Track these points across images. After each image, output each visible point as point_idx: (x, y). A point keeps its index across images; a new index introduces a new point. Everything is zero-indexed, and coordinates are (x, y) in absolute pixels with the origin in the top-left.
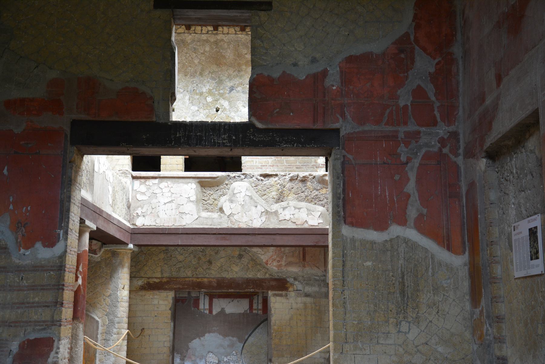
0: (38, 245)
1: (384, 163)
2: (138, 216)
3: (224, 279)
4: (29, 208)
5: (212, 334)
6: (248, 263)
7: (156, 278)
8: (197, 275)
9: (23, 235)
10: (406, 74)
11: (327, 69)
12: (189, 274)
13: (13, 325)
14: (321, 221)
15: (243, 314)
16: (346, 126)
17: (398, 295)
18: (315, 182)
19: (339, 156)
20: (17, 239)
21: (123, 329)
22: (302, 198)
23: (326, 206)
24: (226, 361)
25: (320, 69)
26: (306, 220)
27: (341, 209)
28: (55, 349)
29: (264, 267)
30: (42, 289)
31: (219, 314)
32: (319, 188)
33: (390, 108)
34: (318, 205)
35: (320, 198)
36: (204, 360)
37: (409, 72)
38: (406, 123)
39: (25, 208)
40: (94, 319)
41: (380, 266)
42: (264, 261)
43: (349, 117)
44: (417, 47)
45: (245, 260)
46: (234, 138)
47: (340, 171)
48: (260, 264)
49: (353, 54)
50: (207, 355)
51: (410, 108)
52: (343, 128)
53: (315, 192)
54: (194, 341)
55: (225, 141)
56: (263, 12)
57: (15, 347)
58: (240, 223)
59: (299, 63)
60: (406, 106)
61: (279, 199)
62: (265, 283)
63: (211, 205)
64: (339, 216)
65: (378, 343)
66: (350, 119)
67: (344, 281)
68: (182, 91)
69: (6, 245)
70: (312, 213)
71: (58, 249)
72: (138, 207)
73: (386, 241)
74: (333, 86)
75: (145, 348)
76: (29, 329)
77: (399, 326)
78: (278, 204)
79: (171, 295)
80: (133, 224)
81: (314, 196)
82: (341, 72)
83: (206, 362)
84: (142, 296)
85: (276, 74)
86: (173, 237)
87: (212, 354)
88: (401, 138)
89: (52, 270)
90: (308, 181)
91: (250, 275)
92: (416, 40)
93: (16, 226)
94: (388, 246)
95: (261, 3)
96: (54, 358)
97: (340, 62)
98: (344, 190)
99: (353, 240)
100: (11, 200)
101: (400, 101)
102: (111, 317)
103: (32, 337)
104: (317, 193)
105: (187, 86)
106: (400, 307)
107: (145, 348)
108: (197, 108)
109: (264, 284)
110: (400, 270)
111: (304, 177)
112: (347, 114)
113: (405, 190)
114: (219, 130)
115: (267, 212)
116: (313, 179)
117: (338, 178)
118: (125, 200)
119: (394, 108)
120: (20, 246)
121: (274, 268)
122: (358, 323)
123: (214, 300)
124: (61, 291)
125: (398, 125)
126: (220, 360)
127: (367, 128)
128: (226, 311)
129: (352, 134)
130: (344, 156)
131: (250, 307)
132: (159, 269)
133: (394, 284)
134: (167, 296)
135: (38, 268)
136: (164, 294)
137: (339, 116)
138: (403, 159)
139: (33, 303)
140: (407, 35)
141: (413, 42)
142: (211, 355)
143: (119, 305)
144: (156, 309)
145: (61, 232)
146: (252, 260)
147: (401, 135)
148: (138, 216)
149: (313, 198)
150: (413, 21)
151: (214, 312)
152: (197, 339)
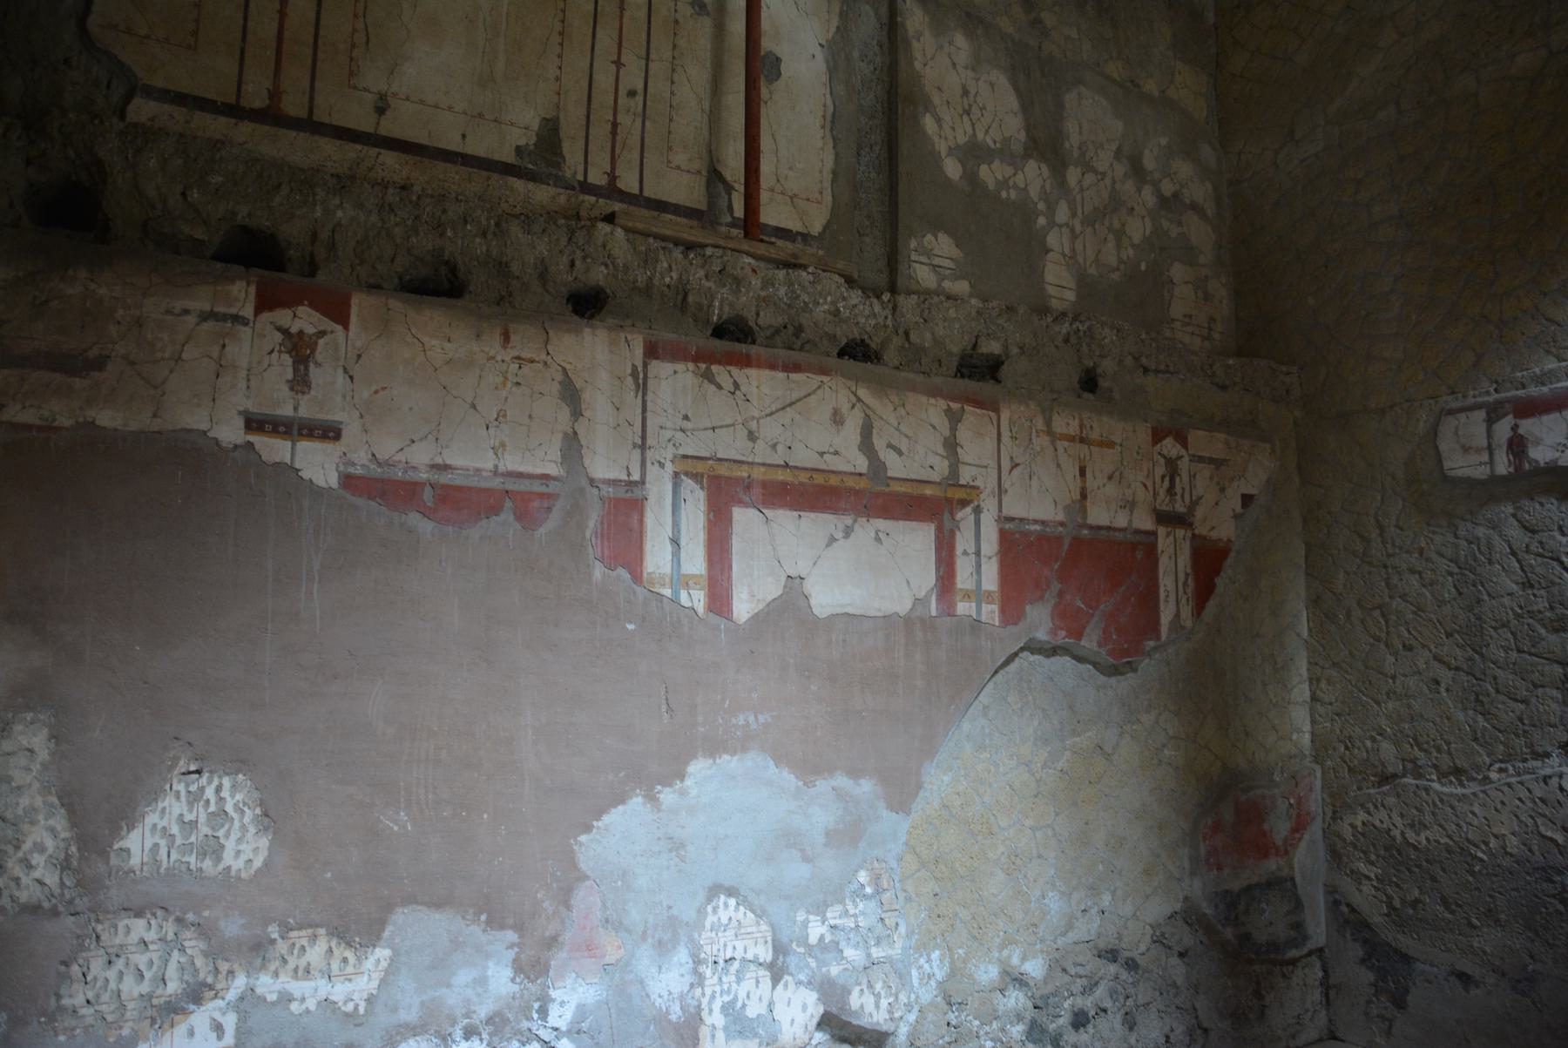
5: (730, 762)
15: (908, 621)
24: (822, 938)
50: (701, 912)
54: (615, 818)
83: (698, 962)
87: (732, 902)
123: (744, 518)
126: (785, 940)
128: (813, 602)
131: (939, 578)
152: (637, 802)
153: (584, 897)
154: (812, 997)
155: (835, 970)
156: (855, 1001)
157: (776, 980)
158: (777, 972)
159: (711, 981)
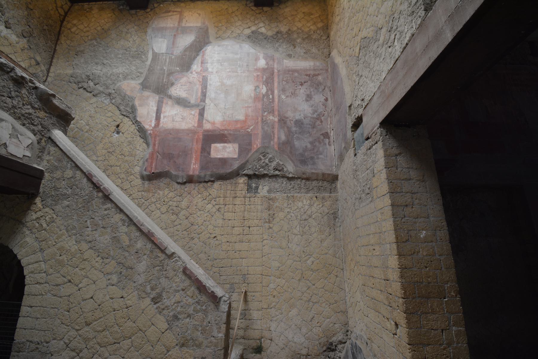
14: (28, 154)
18: (34, 96)
22: (5, 105)
23: (37, 135)
26: (5, 144)
32: (36, 106)
34: (27, 128)
35: (33, 120)
53: (29, 109)
70: (19, 136)
81: (26, 113)
90: (25, 87)
104: (31, 111)
111: (22, 77)
116: (33, 89)
149: (23, 115)
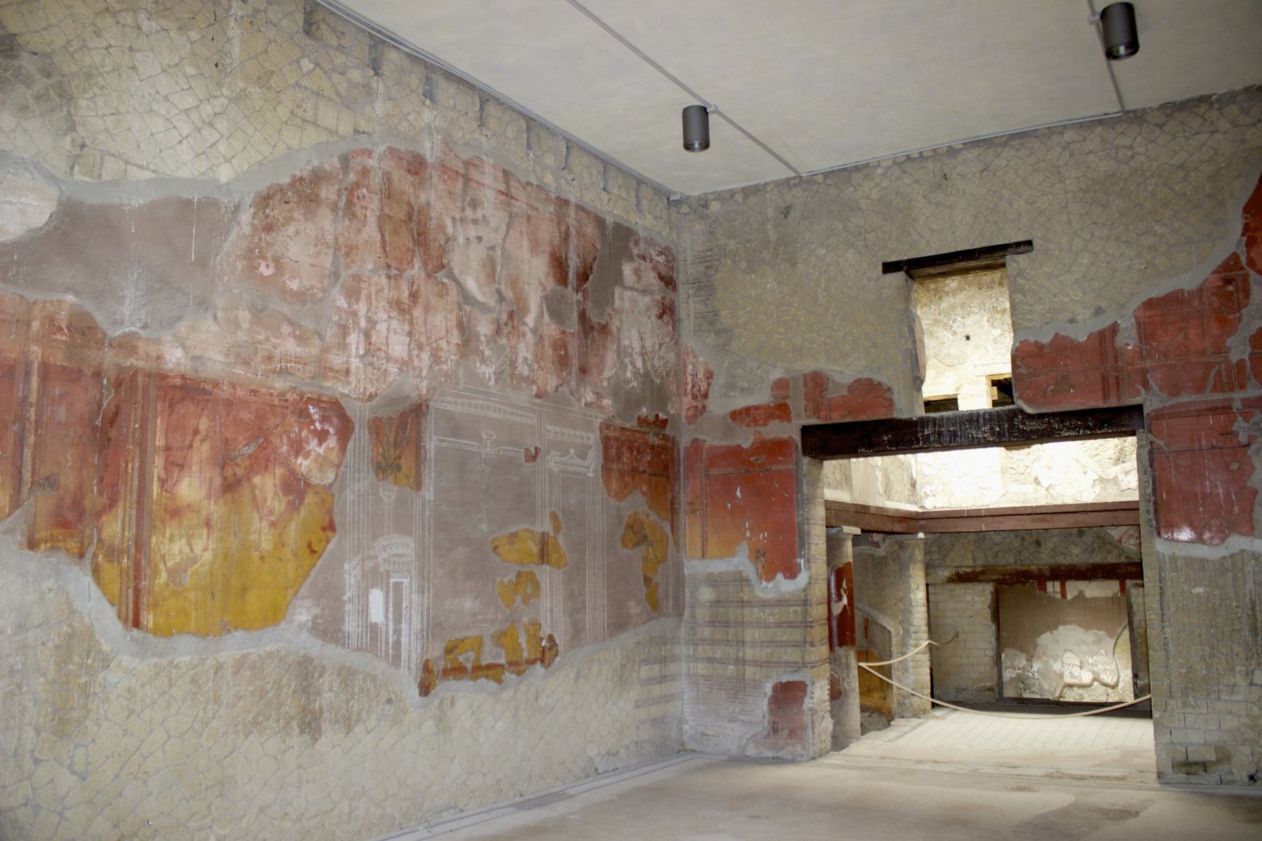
0: (780, 576)
1: (1213, 447)
2: (927, 495)
3: (1059, 566)
4: (766, 535)
5: (1067, 626)
6: (1093, 542)
7: (967, 567)
8: (1021, 561)
9: (763, 566)
10: (1238, 315)
11: (1116, 322)
12: (1011, 560)
13: (764, 665)
15: (1112, 598)
16: (1151, 400)
17: (1247, 634)
19: (1144, 442)
20: (757, 570)
21: (922, 639)
25: (1108, 323)
27: (1152, 516)
28: (809, 694)
29: (1117, 547)
30: (789, 627)
31: (1075, 599)
33: (1217, 367)
36: (1059, 661)
37: (1244, 311)
38: (1242, 386)
39: (761, 535)
40: (885, 628)
41: (1216, 592)
42: (1116, 538)
43: (1154, 386)
44: (1252, 273)
45: (1089, 537)
46: (998, 429)
47: (1147, 464)
48: (1111, 543)
49: (1153, 295)
51: (1248, 364)
52: (1148, 403)
54: (1044, 635)
55: (986, 435)
56: (1022, 256)
57: (768, 688)
58: (1065, 498)
59: (1078, 318)
60: (1241, 363)
61: (1118, 460)
62: (1121, 569)
63: (1022, 474)
64: (1151, 526)
65: (1219, 699)
66: (1157, 389)
67: (1163, 615)
68: (976, 310)
69: (748, 576)
71: (802, 579)
72: (926, 484)
73: (1224, 558)
74: (1128, 345)
75: (961, 657)
76: (781, 670)
77: (1250, 677)
78: (1118, 467)
79: (989, 588)
80: (922, 507)
82: (1138, 324)
83: (1063, 663)
84: (950, 590)
85: (1046, 339)
86: (974, 520)
88: (1238, 409)
89: (798, 605)
91: (1097, 559)
92: (1251, 263)
93: (756, 555)
94: (1228, 563)
95: (1018, 244)
96: (809, 703)
97: (1136, 310)
98: (1154, 490)
99: (1174, 559)
100: (747, 526)
101: (1231, 355)
102: (906, 625)
103: (784, 680)
105: (984, 304)
106: (1251, 650)
107: (961, 657)
108: (999, 332)
109: (1119, 571)
110: (1247, 598)
112: (1151, 382)
113: (1248, 484)
114: (978, 421)
115: (1102, 480)
117: (1146, 473)
118: (906, 478)
119: (1223, 366)
120: (761, 578)
121: (1132, 547)
122: (1188, 672)
124: (809, 629)
125: (1232, 389)
127: (1184, 398)
129: (1161, 410)
130: (1151, 443)
132: (970, 555)
133: (1239, 618)
134: (984, 590)
135: (782, 602)
136: (979, 587)
137: (1139, 387)
138: (1243, 438)
139: (781, 642)
140: (1235, 257)
141: (1246, 267)
142: (1069, 654)
143: (913, 611)
144: (970, 607)
145: (802, 561)
146: (1098, 537)
147: (1237, 405)
148: (927, 495)
150: (1243, 235)
151: (1069, 597)
152: (1048, 633)
153: (1037, 649)
154: (1090, 674)
155: (1096, 669)
156: (1102, 676)
157: (1081, 668)
158: (1081, 668)
159: (1066, 667)
